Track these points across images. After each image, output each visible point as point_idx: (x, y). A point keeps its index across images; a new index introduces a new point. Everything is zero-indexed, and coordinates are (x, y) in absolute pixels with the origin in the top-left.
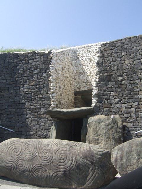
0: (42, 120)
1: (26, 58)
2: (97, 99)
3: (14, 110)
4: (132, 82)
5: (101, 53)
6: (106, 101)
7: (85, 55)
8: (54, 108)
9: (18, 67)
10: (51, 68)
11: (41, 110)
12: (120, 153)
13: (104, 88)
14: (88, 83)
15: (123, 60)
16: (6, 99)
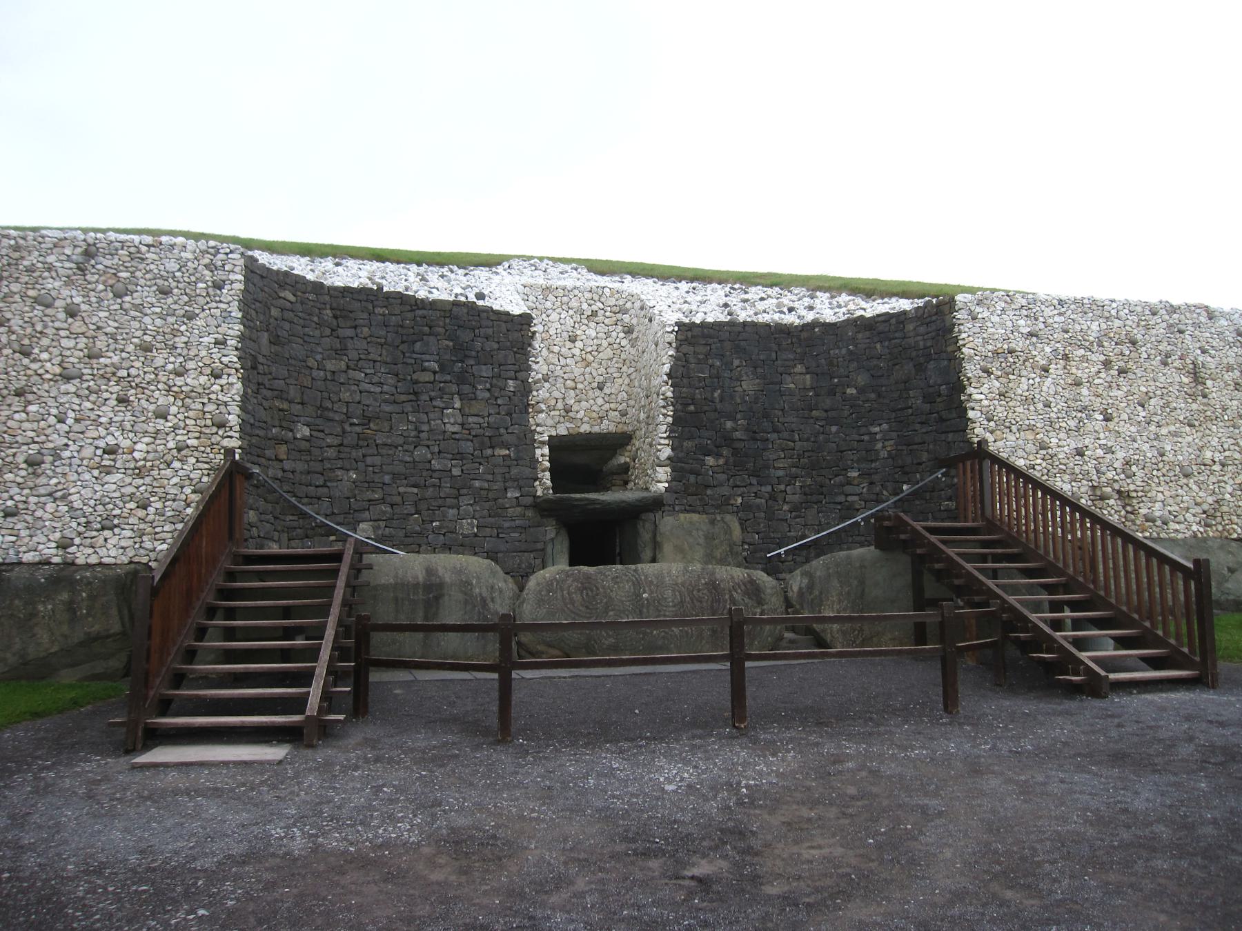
0: (513, 524)
1: (448, 321)
2: (668, 469)
3: (415, 490)
4: (758, 436)
5: (677, 349)
6: (692, 479)
7: (554, 316)
8: (547, 488)
9: (418, 345)
10: (534, 366)
11: (509, 495)
12: (806, 581)
13: (688, 444)
14: (571, 414)
15: (737, 380)
16: (384, 451)
